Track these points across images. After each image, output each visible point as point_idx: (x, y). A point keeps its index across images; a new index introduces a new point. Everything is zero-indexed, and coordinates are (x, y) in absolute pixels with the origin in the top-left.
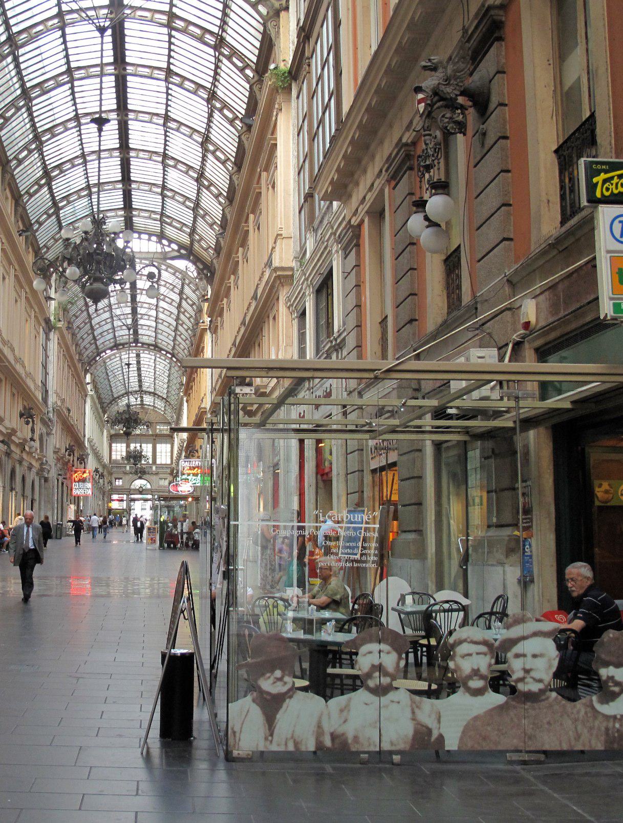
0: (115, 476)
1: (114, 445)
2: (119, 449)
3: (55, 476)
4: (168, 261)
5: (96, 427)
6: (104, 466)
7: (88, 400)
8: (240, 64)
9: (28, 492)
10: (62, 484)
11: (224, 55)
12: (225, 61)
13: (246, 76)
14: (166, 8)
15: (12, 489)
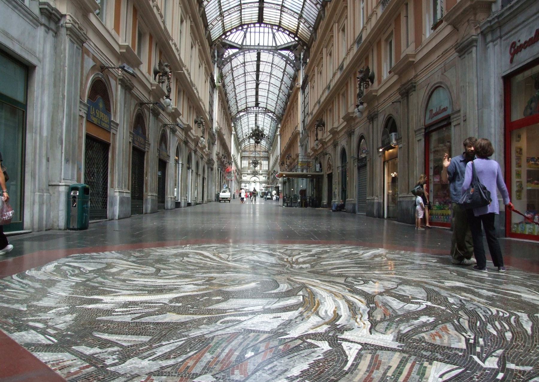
0: (243, 175)
1: (243, 161)
2: (245, 163)
3: (217, 168)
4: (279, 51)
5: (236, 151)
6: (239, 170)
7: (233, 136)
8: (308, 26)
9: (201, 172)
10: (221, 173)
11: (302, 22)
12: (302, 24)
13: (310, 30)
14: (281, 3)
15: (189, 168)
